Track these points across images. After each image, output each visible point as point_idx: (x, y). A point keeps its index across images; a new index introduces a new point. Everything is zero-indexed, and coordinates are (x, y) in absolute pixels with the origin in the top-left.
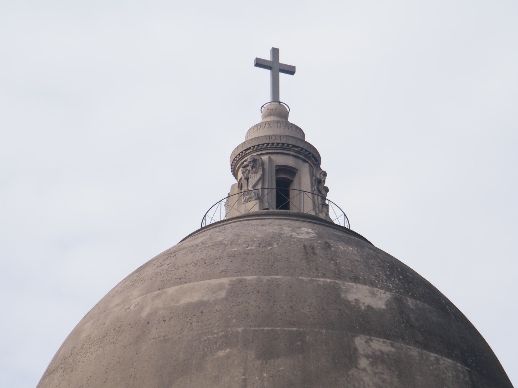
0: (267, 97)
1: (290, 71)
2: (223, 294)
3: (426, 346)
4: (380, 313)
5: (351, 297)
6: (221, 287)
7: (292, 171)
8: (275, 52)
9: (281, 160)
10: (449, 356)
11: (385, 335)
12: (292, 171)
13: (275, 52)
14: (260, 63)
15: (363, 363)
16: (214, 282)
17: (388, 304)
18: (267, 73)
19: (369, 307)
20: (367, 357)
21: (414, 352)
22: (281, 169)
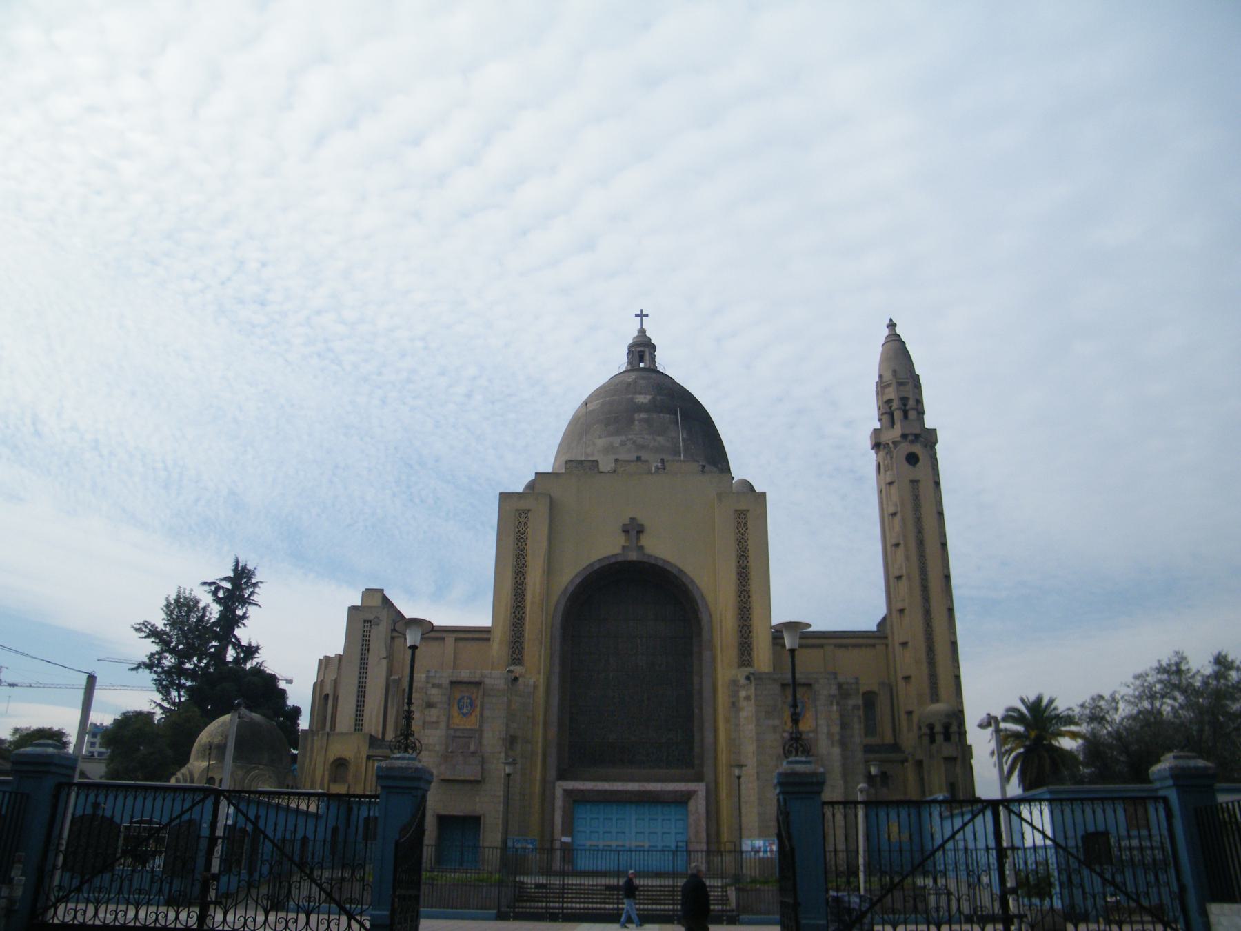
0: (639, 327)
1: (647, 315)
2: (599, 406)
3: (660, 412)
4: (646, 404)
5: (637, 400)
6: (598, 403)
7: (643, 352)
8: (642, 310)
9: (642, 349)
10: (669, 414)
11: (647, 411)
12: (643, 352)
13: (642, 310)
14: (636, 315)
15: (636, 423)
16: (598, 401)
17: (649, 401)
18: (639, 318)
19: (642, 403)
20: (638, 420)
21: (655, 415)
22: (640, 352)
